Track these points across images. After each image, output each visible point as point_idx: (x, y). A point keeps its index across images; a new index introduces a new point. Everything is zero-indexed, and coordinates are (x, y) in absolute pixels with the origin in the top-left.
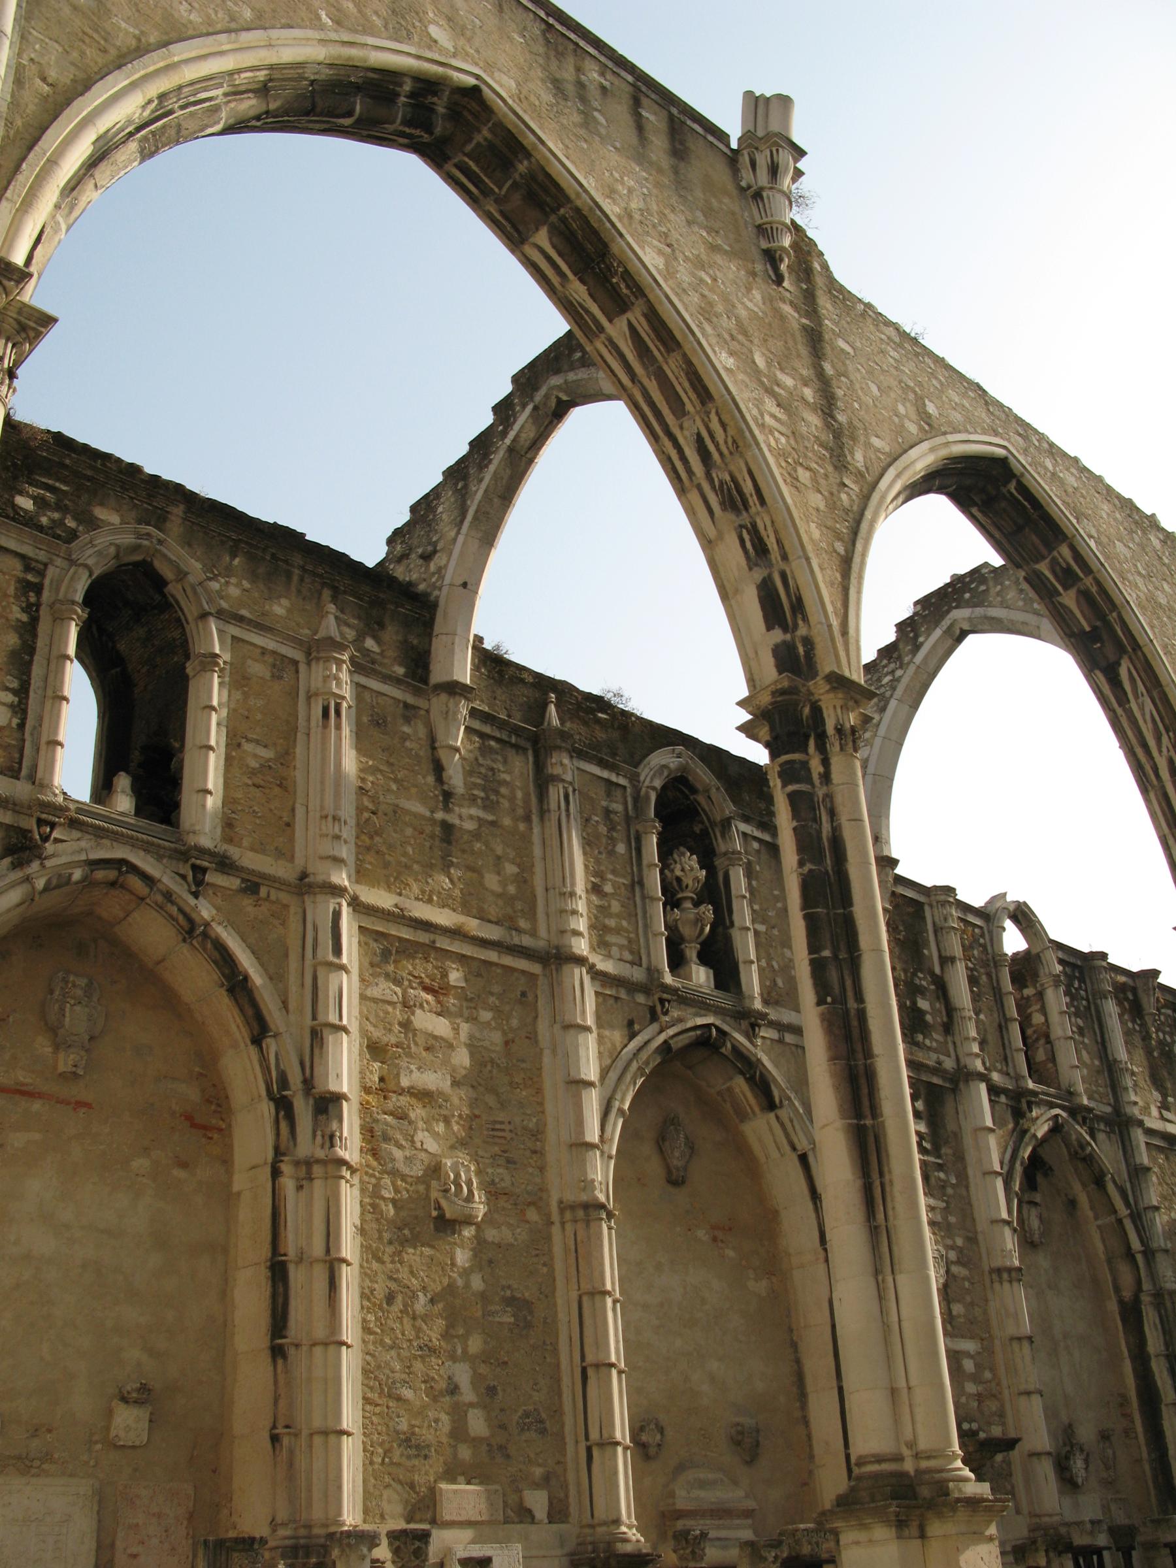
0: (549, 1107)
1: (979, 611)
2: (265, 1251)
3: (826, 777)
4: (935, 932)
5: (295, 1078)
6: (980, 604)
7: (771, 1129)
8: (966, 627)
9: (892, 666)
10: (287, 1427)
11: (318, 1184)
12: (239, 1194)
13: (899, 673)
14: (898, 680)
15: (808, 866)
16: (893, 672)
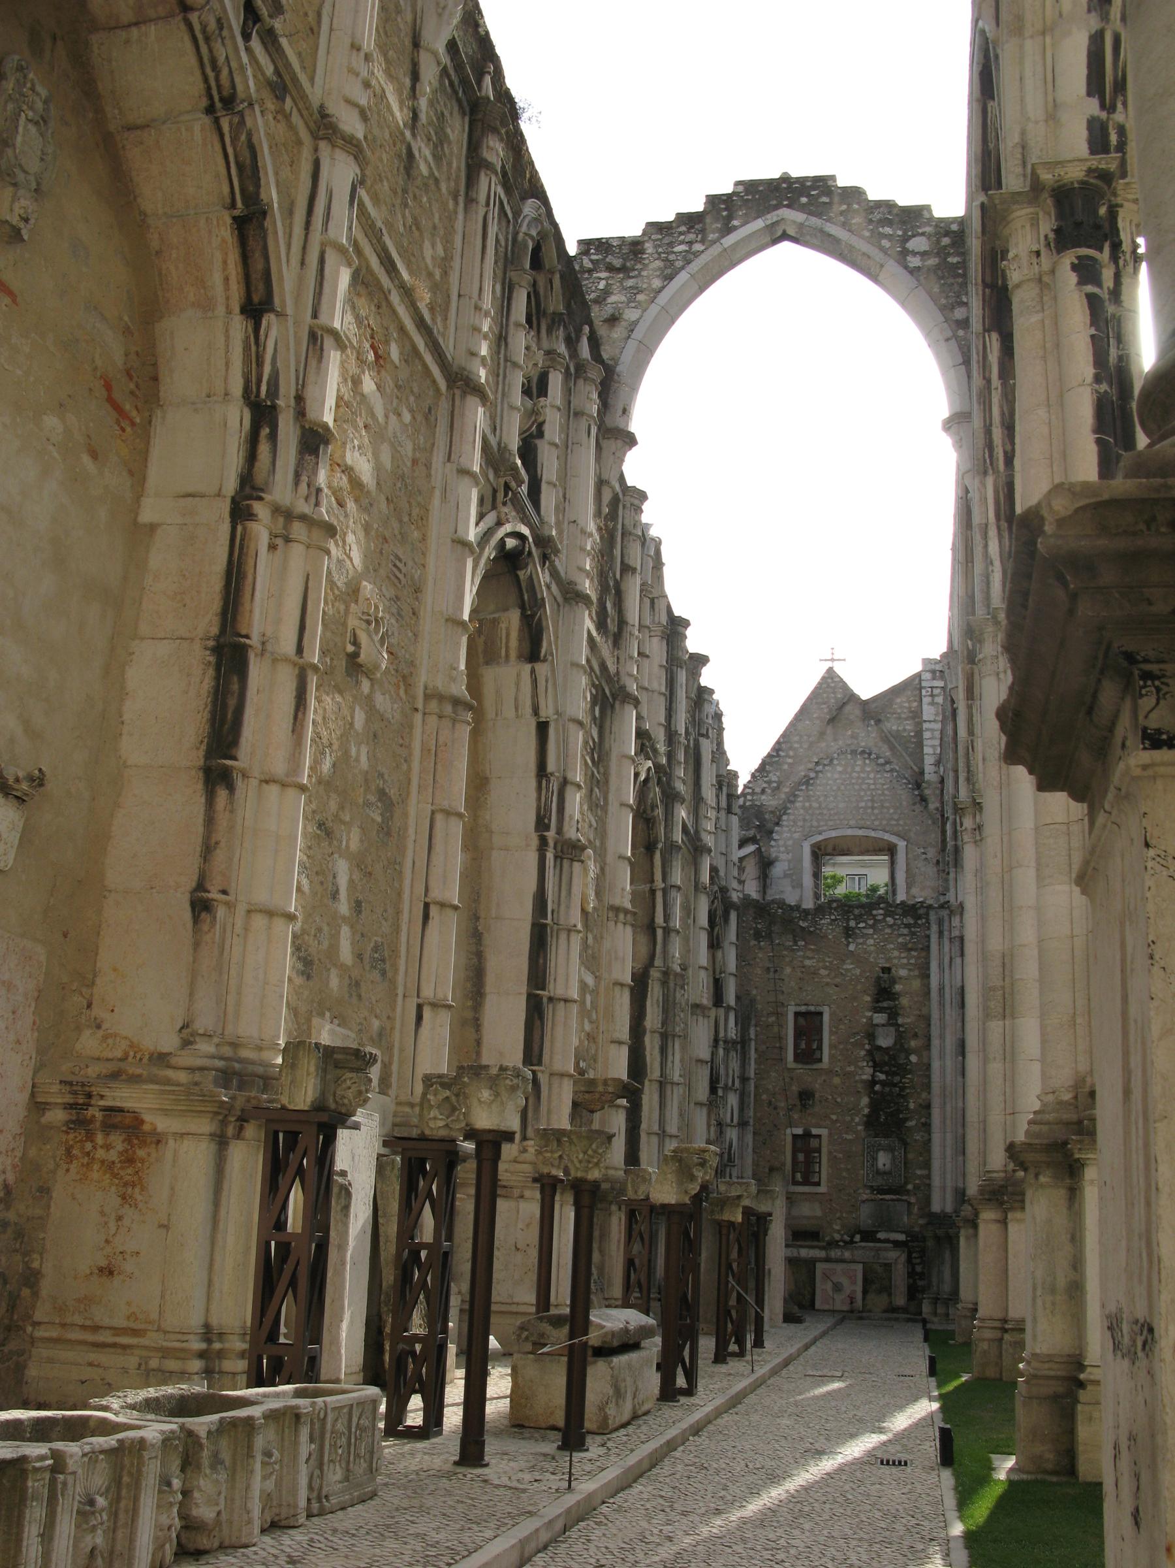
0: (431, 561)
1: (814, 221)
2: (208, 623)
3: (1116, 294)
4: (623, 534)
5: (287, 390)
6: (819, 215)
7: (518, 684)
8: (791, 232)
9: (691, 237)
10: (224, 892)
11: (297, 550)
12: (152, 528)
13: (698, 247)
14: (697, 254)
15: (1104, 387)
16: (690, 243)
